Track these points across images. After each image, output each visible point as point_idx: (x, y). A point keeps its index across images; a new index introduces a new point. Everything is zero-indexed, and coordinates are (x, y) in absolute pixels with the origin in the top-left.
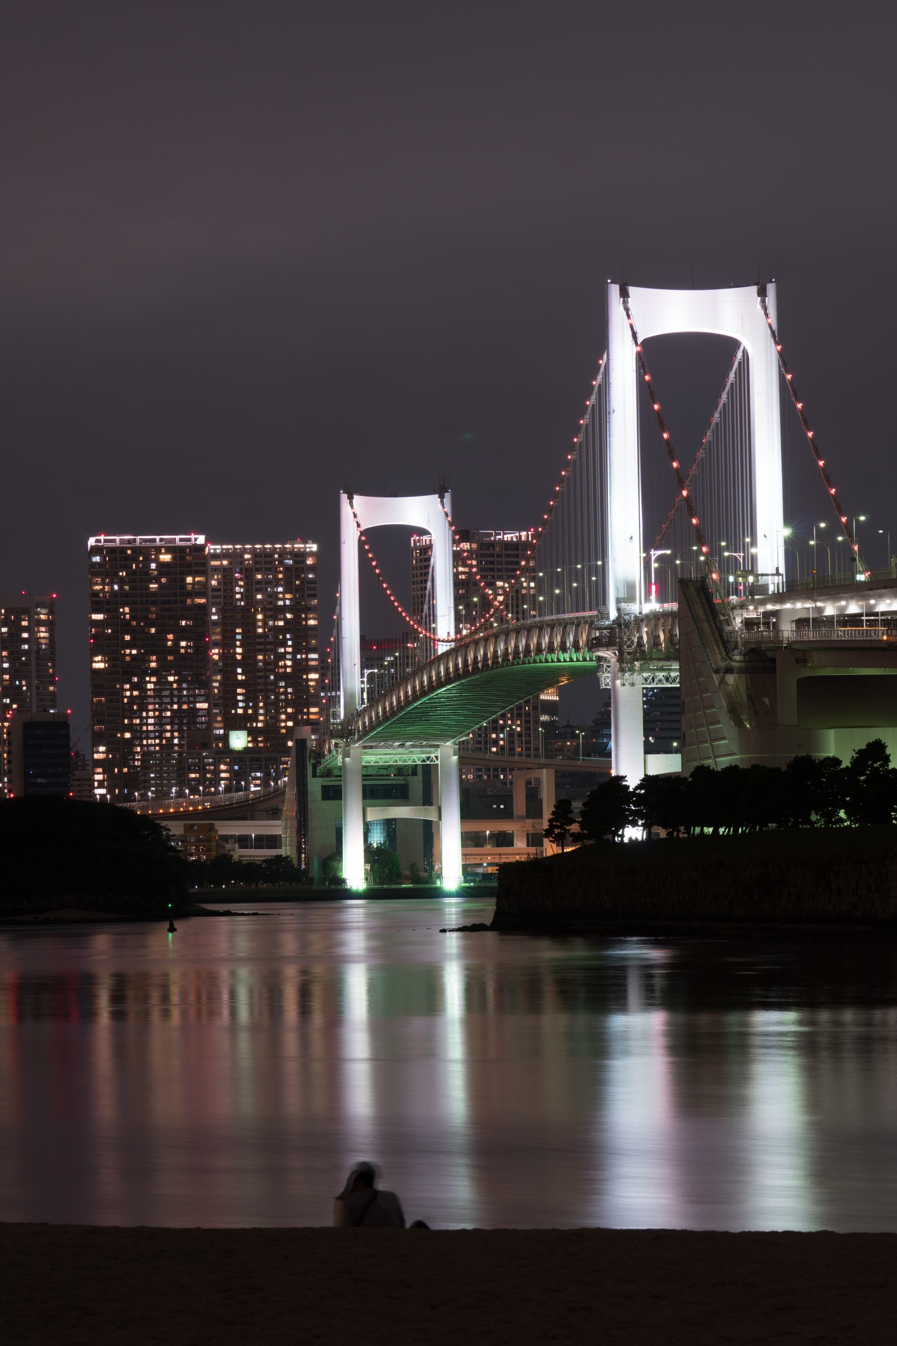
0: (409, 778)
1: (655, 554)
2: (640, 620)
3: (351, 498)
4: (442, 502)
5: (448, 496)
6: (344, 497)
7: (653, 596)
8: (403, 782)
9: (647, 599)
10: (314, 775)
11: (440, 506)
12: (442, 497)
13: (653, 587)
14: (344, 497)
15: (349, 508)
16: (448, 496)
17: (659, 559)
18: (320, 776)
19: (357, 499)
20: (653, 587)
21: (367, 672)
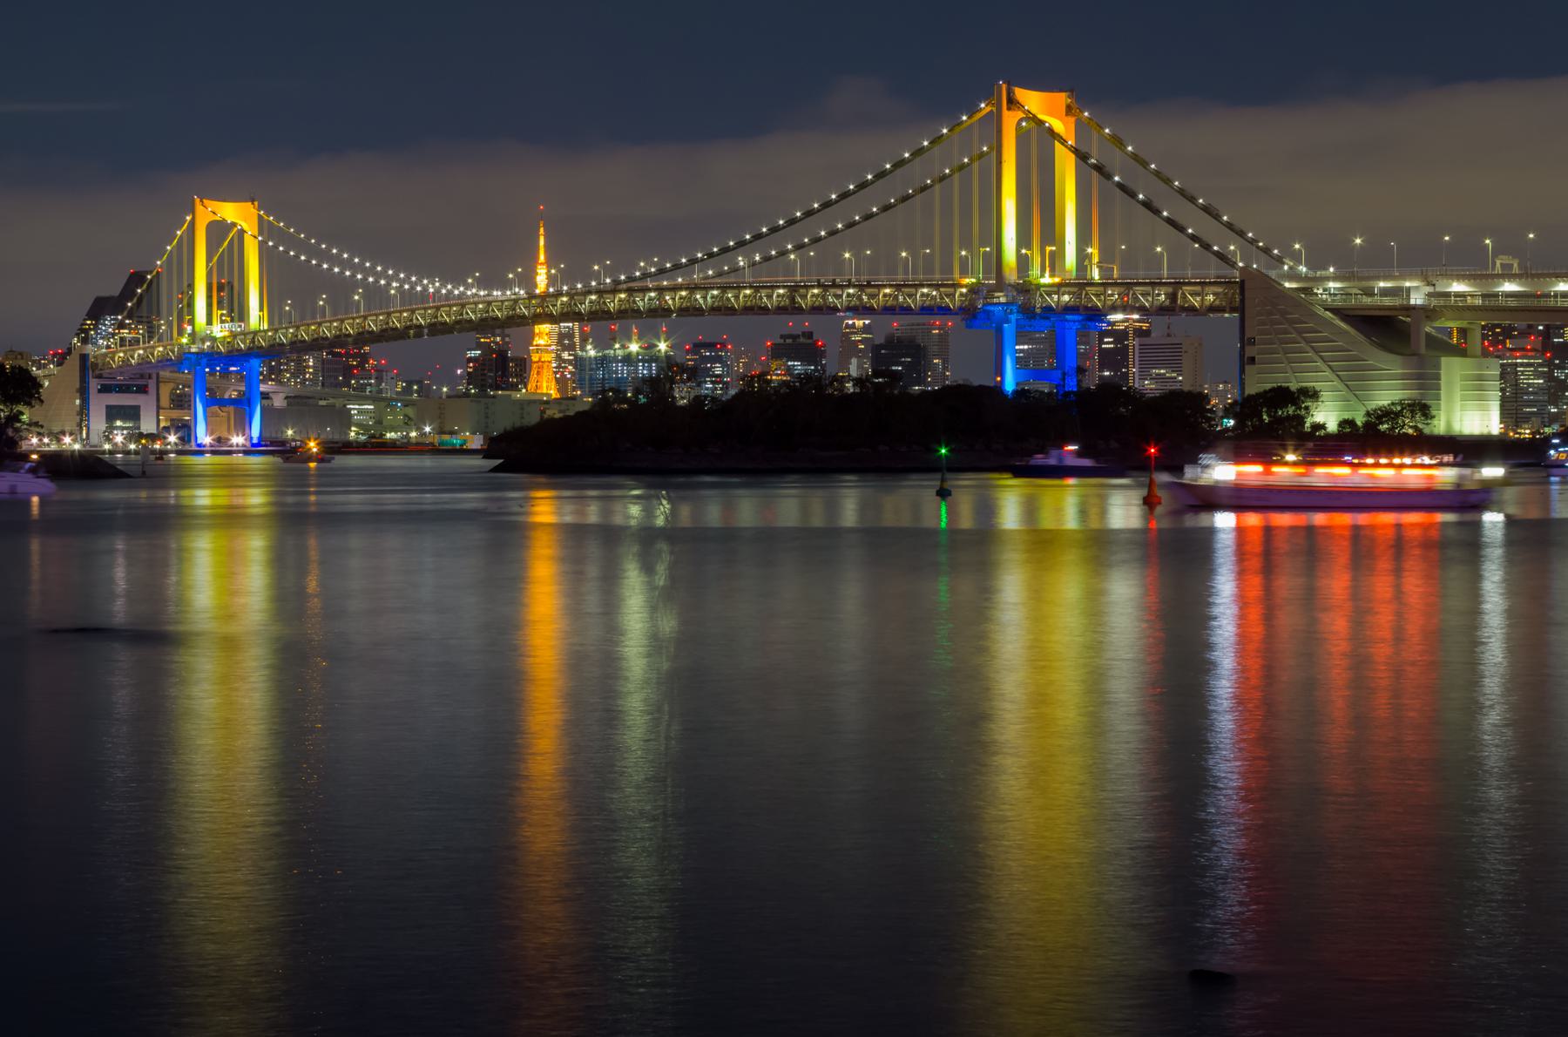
0: (150, 381)
1: (1048, 249)
2: (1038, 286)
3: (201, 201)
4: (254, 207)
5: (256, 203)
6: (197, 201)
7: (1047, 274)
8: (145, 383)
9: (1042, 276)
10: (93, 378)
11: (252, 210)
12: (253, 204)
13: (1048, 269)
14: (197, 201)
15: (201, 207)
16: (256, 203)
17: (1051, 252)
18: (96, 377)
19: (204, 200)
20: (1048, 269)
21: (220, 312)
